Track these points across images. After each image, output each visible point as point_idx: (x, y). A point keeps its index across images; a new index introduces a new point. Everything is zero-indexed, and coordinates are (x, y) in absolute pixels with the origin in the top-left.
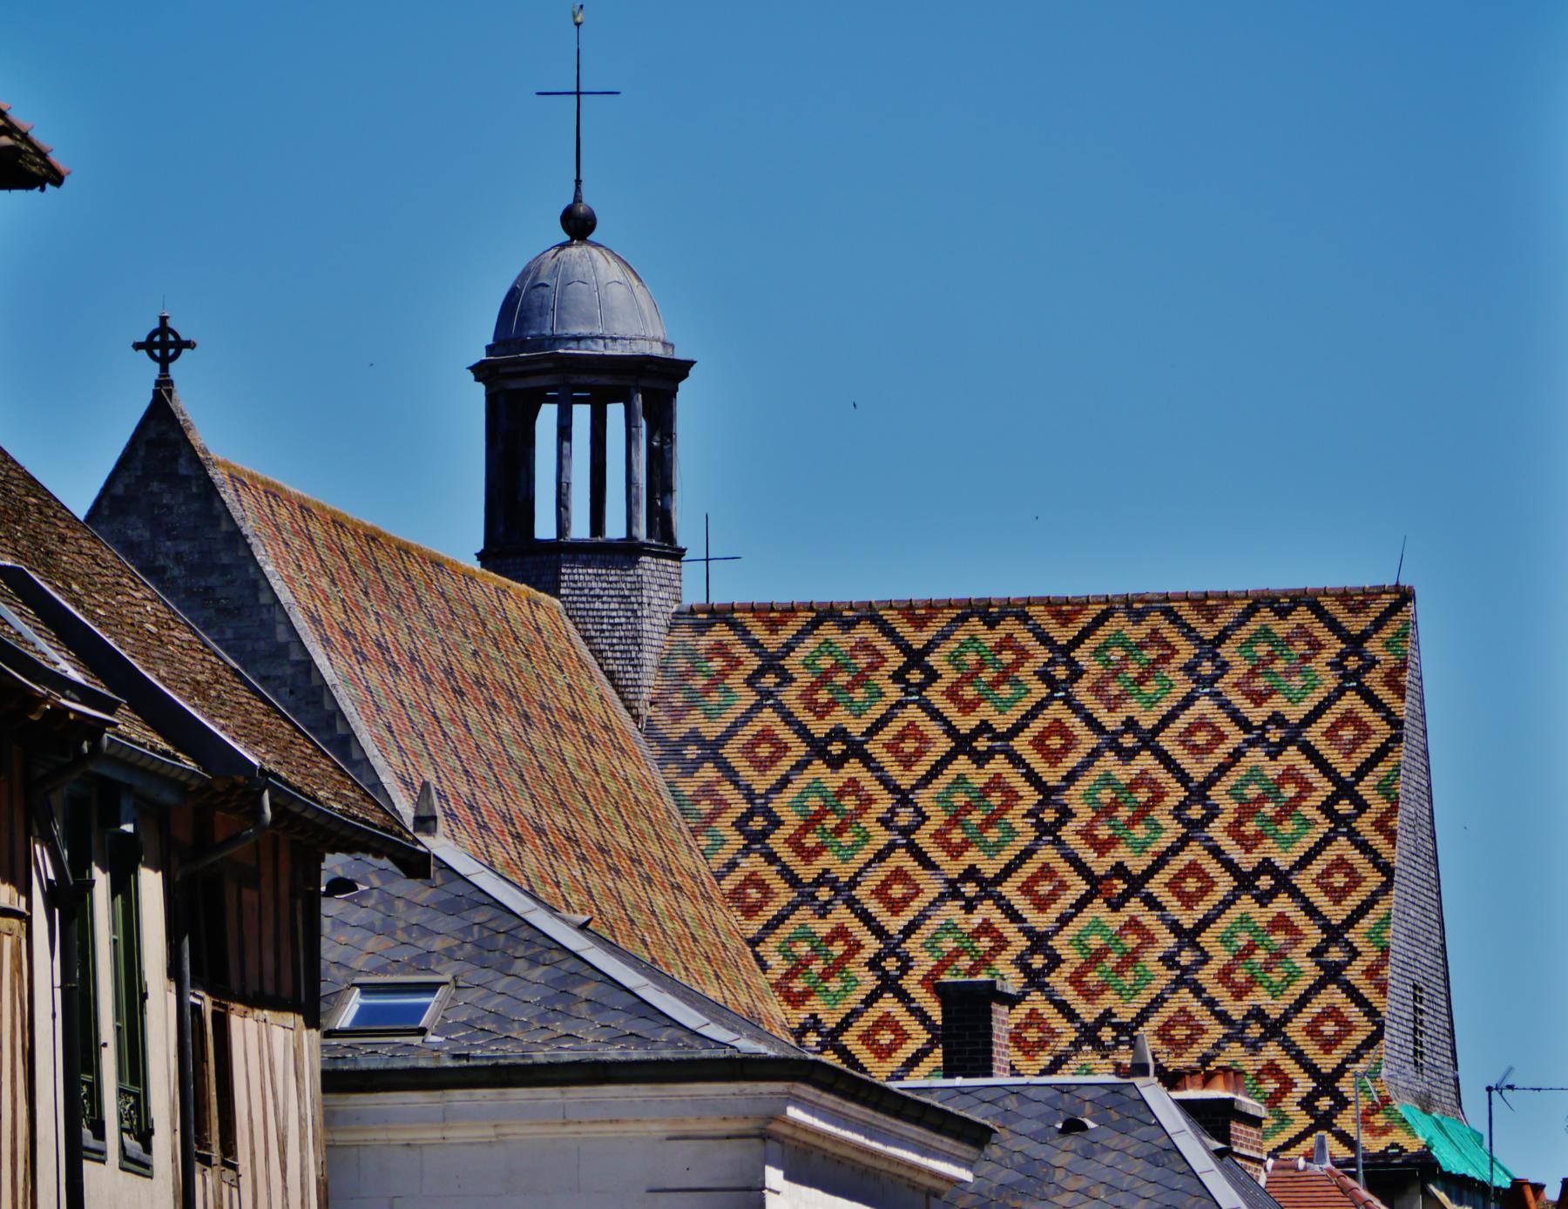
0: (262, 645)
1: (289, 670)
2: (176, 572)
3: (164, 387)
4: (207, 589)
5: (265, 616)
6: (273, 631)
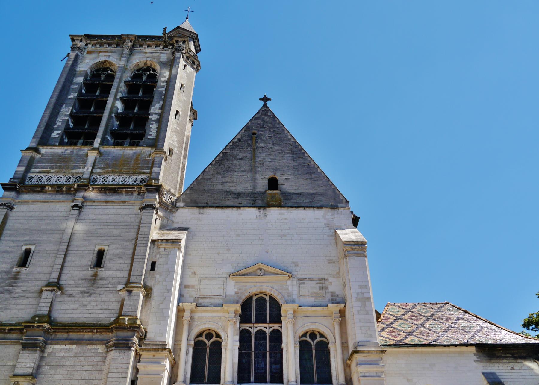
0: (285, 139)
1: (291, 142)
2: (268, 128)
3: (265, 105)
4: (274, 130)
5: (286, 134)
6: (288, 136)
